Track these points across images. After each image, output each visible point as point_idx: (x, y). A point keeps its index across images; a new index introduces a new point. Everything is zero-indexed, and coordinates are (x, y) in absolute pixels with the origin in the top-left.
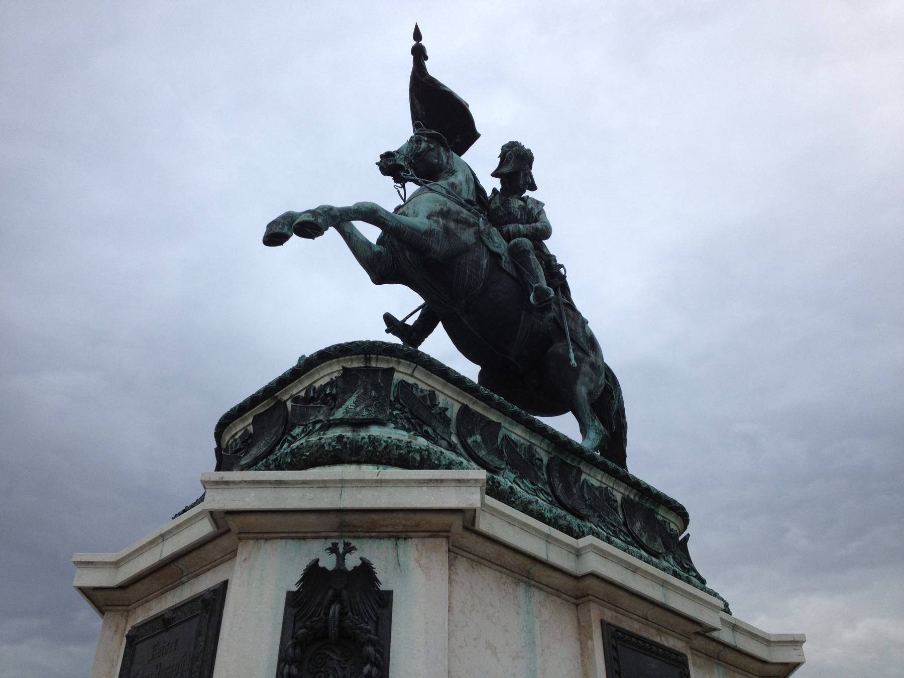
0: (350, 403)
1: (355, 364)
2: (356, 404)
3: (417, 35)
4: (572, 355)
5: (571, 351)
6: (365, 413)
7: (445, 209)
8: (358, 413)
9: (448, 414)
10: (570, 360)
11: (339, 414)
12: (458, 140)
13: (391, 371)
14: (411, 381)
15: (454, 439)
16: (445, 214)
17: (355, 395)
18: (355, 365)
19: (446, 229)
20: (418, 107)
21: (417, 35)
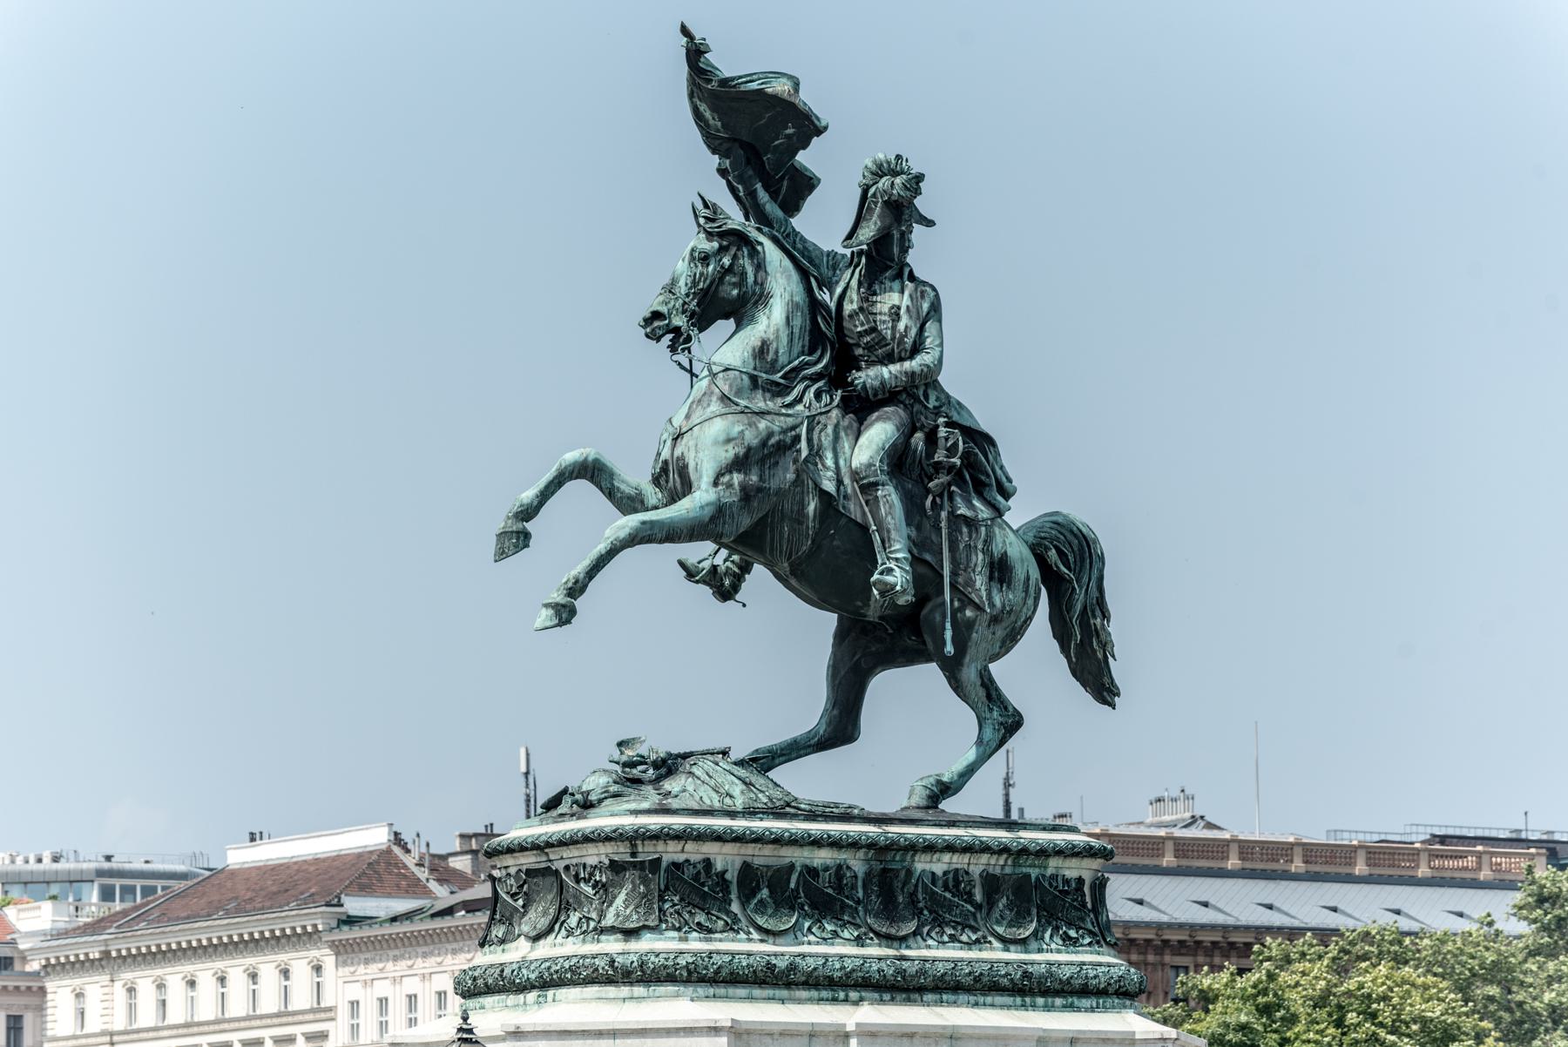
0: (619, 901)
1: (621, 852)
2: (626, 905)
3: (685, 31)
4: (948, 635)
5: (948, 625)
6: (635, 917)
7: (741, 451)
8: (627, 918)
9: (728, 876)
10: (944, 643)
11: (609, 920)
12: (790, 131)
13: (659, 860)
14: (681, 858)
15: (735, 907)
16: (739, 464)
17: (624, 892)
18: (622, 850)
19: (747, 495)
20: (708, 115)
21: (685, 31)
